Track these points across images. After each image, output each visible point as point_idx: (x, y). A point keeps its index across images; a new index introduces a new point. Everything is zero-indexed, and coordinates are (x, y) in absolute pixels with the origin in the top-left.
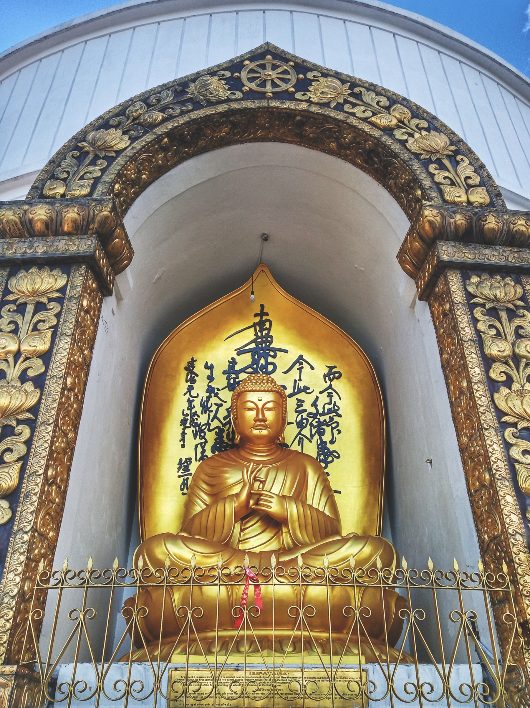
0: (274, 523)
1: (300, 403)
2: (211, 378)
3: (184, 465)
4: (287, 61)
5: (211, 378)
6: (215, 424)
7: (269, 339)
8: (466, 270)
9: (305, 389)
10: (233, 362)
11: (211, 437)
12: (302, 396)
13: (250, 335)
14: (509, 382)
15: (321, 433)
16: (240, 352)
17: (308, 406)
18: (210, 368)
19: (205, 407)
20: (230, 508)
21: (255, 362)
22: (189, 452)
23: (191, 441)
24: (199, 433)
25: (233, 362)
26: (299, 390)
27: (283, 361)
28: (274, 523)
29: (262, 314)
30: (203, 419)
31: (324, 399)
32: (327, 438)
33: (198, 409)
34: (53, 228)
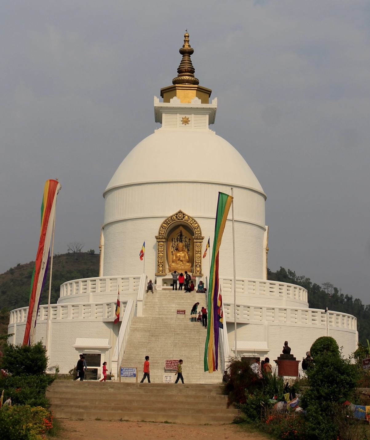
0: (182, 261)
1: (186, 243)
2: (175, 240)
3: (172, 252)
4: (182, 213)
5: (175, 240)
6: (175, 246)
7: (182, 234)
8: (196, 242)
9: (186, 241)
10: (177, 238)
11: (175, 248)
12: (186, 242)
13: (180, 234)
14: (197, 253)
15: (188, 247)
16: (178, 236)
17: (186, 244)
18: (175, 239)
19: (174, 244)
20: (178, 259)
21: (180, 237)
22: (172, 250)
23: (173, 249)
24: (174, 248)
25: (177, 238)
26: (185, 241)
27: (184, 237)
28: (182, 261)
29: (181, 231)
30: (174, 246)
31: (188, 243)
32: (189, 248)
33: (173, 245)
34: (162, 239)
